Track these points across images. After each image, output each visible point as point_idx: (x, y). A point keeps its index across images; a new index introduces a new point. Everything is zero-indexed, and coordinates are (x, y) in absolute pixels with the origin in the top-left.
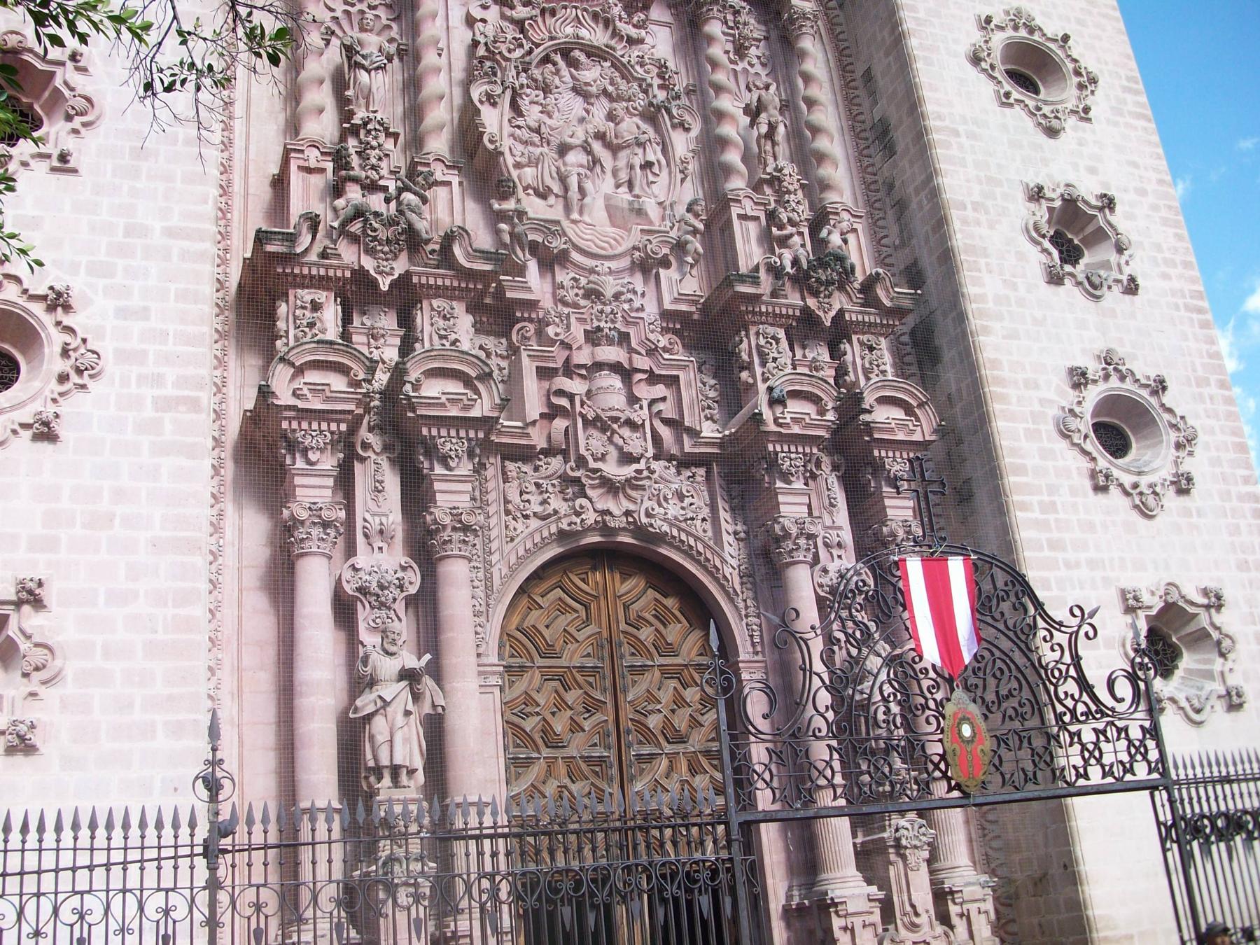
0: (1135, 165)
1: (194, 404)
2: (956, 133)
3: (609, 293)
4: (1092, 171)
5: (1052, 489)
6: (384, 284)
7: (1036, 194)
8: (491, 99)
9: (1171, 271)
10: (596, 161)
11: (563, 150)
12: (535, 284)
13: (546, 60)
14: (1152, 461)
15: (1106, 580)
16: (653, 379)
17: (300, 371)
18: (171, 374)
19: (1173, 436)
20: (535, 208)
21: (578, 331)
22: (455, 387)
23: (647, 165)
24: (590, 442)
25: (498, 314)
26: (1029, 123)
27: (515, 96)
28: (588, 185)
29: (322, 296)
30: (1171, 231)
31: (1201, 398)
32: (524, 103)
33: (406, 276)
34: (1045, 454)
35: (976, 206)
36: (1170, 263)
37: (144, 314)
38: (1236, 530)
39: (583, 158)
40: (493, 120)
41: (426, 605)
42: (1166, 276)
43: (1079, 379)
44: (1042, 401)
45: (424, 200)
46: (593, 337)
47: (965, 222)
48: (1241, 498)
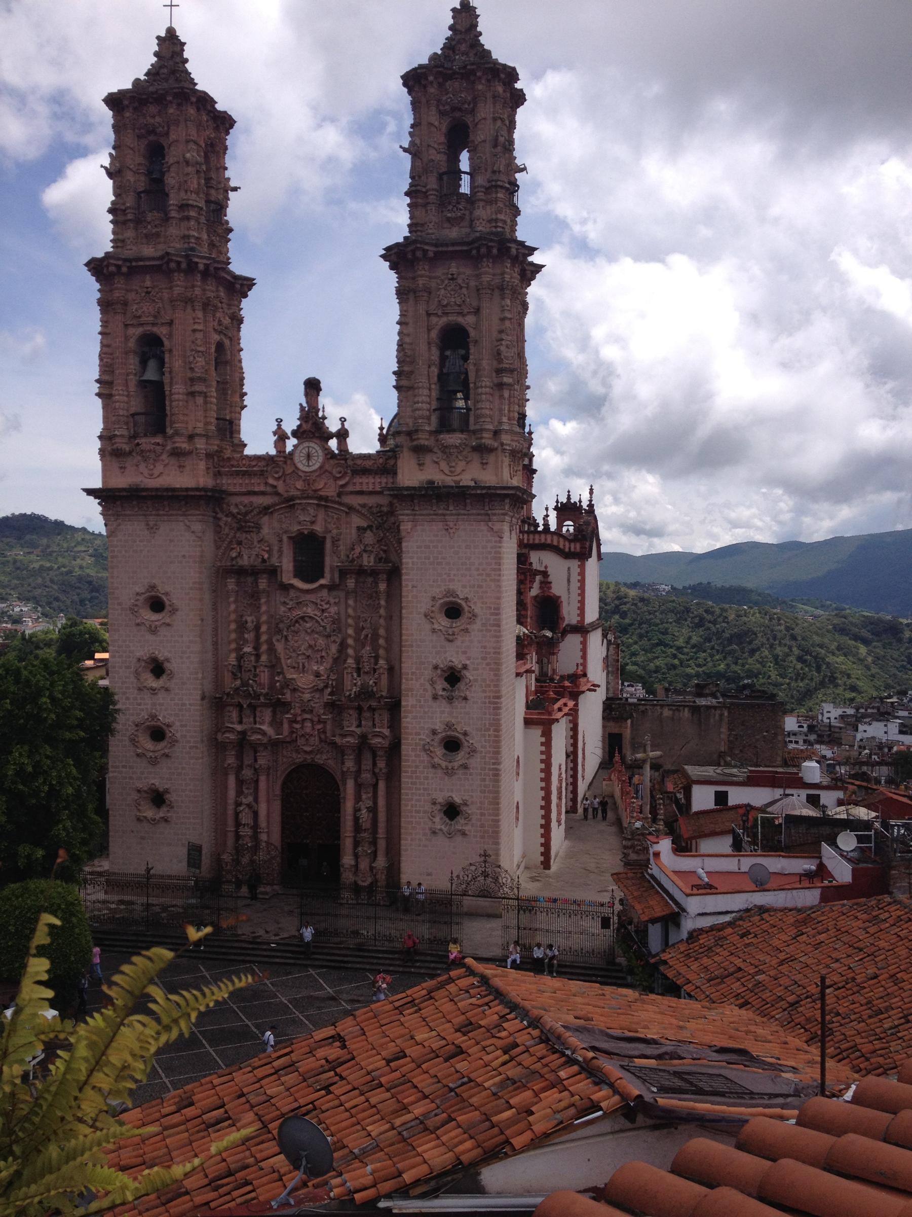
0: (485, 647)
1: (197, 747)
2: (412, 646)
3: (306, 700)
4: (465, 653)
5: (417, 767)
6: (245, 706)
7: (436, 667)
8: (278, 640)
9: (487, 689)
10: (308, 656)
11: (299, 655)
12: (288, 696)
13: (297, 622)
14: (460, 757)
15: (429, 794)
16: (319, 722)
17: (224, 733)
18: (192, 740)
19: (468, 750)
20: (291, 675)
21: (299, 711)
22: (259, 737)
23: (322, 657)
24: (301, 742)
25: (279, 706)
26: (443, 638)
27: (286, 637)
28: (306, 664)
29: (231, 709)
30: (492, 673)
31: (484, 736)
32: (290, 638)
33: (250, 703)
34: (417, 756)
35: (413, 673)
36: (489, 686)
37: (186, 726)
38: (484, 780)
39: (304, 657)
40: (279, 647)
41: (257, 782)
42: (484, 691)
43: (434, 732)
44: (420, 739)
45: (255, 681)
46: (304, 711)
47: (407, 680)
48: (490, 769)
